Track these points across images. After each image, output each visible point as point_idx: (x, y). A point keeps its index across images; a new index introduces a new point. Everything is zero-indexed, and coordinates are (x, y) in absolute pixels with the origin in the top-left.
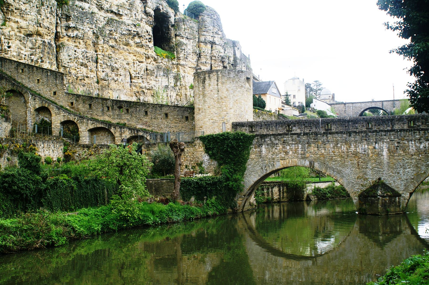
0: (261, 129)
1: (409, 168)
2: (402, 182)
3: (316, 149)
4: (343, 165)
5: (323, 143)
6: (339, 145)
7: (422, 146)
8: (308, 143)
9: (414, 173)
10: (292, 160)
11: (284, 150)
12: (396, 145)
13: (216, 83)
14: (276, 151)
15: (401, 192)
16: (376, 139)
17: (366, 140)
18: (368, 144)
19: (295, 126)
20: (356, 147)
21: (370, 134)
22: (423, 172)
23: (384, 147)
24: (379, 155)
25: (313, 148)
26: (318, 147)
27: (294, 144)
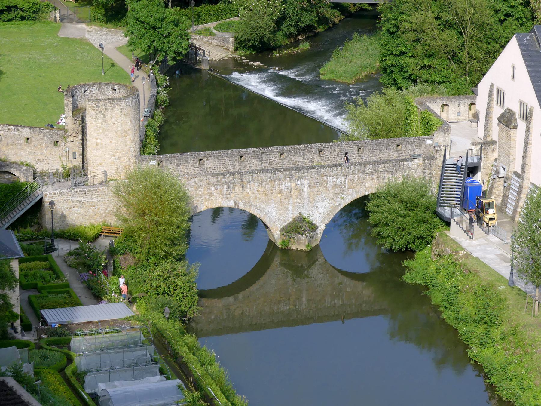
0: (171, 164)
1: (327, 201)
2: (320, 215)
3: (241, 189)
5: (249, 182)
6: (264, 184)
7: (338, 181)
8: (233, 184)
9: (331, 205)
10: (216, 202)
11: (209, 191)
12: (316, 181)
13: (120, 114)
14: (201, 193)
15: (318, 225)
16: (299, 177)
17: (289, 177)
19: (207, 160)
20: (280, 185)
21: (293, 172)
22: (338, 204)
24: (301, 191)
25: (238, 189)
26: (243, 187)
27: (220, 185)
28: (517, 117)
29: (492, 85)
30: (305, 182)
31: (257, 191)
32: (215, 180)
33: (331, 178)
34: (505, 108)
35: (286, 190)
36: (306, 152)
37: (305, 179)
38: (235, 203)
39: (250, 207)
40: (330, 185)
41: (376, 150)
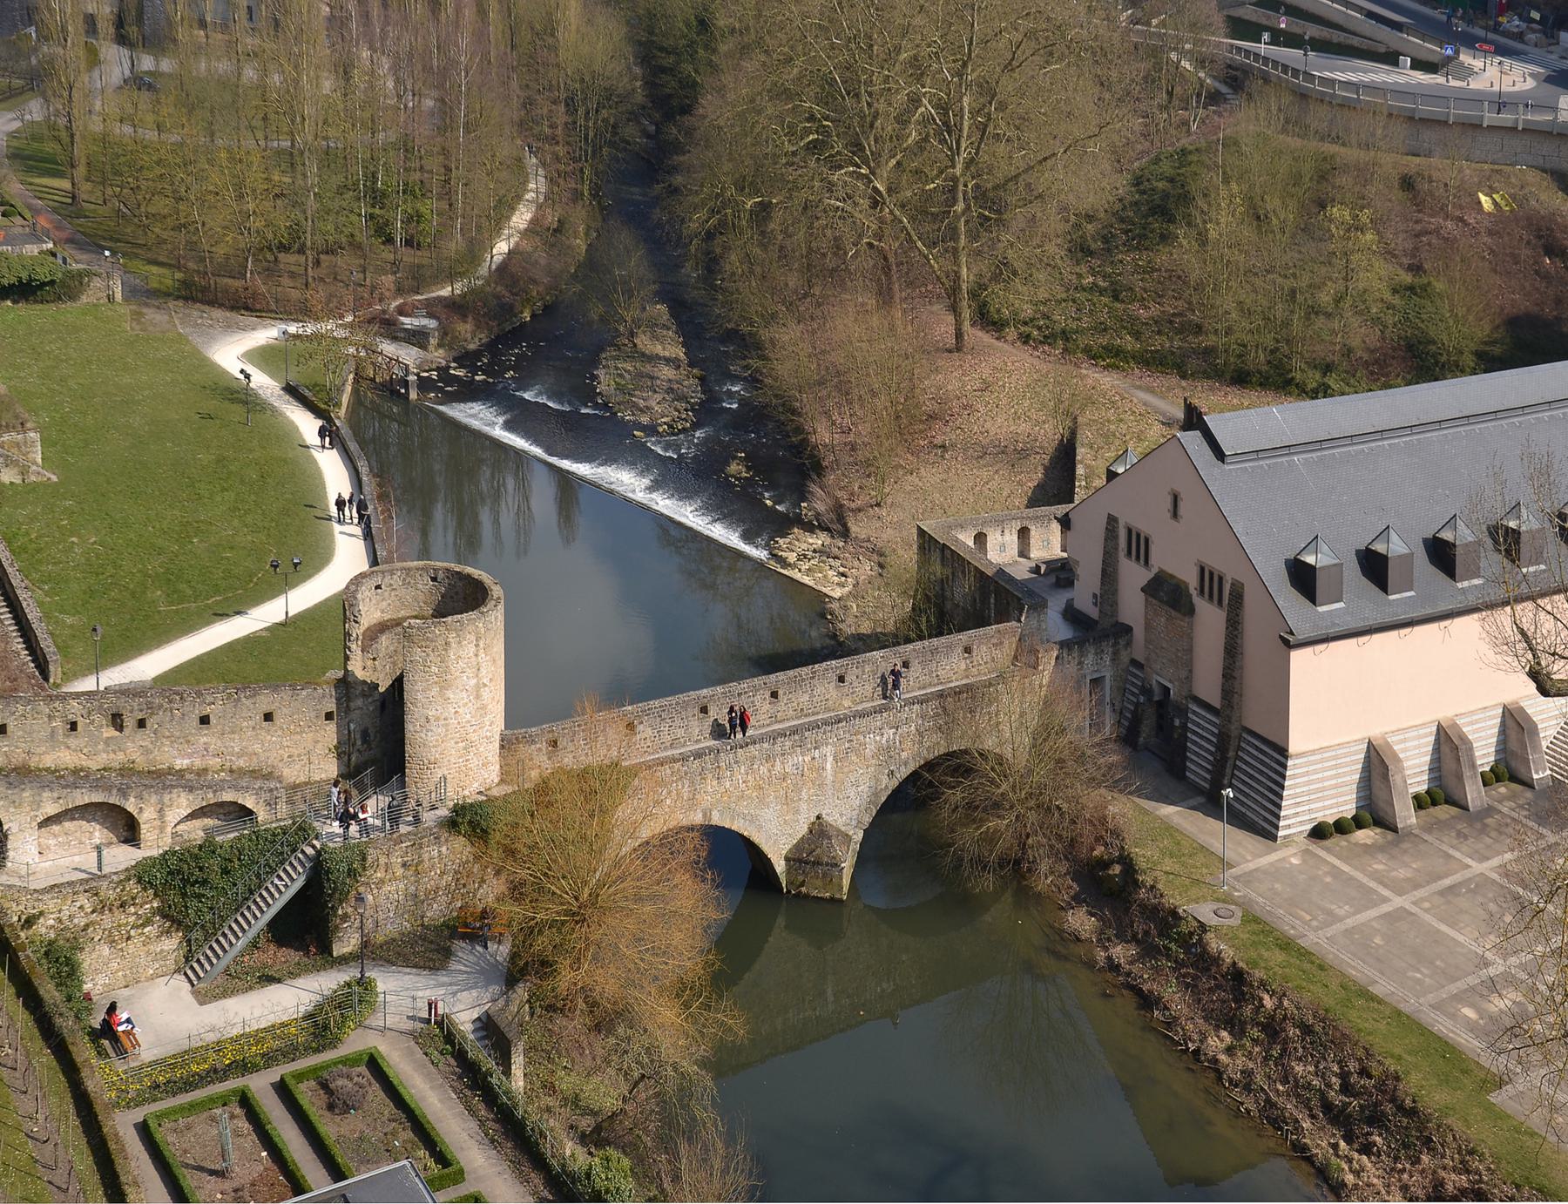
3: (715, 783)
4: (762, 802)
5: (730, 767)
6: (755, 766)
8: (700, 774)
18: (803, 754)
21: (806, 734)
23: (828, 754)
25: (711, 785)
28: (1194, 593)
29: (1112, 521)
30: (828, 750)
31: (744, 782)
32: (669, 772)
33: (872, 736)
34: (1155, 570)
35: (795, 772)
36: (816, 681)
37: (827, 744)
38: (705, 815)
39: (733, 819)
40: (870, 749)
41: (931, 661)
